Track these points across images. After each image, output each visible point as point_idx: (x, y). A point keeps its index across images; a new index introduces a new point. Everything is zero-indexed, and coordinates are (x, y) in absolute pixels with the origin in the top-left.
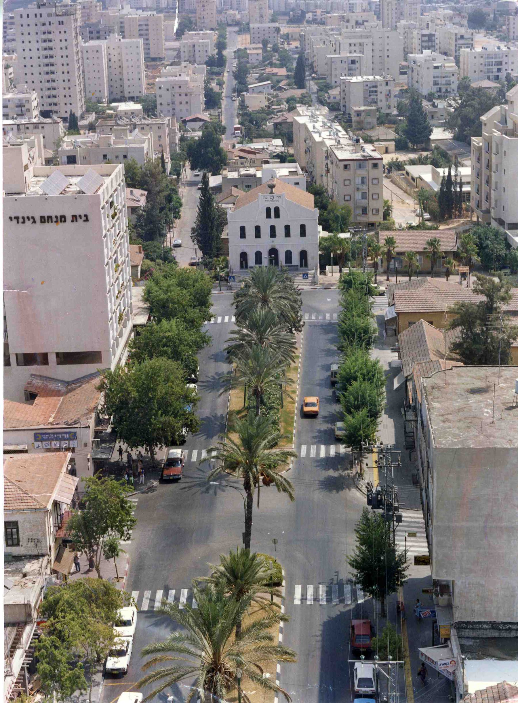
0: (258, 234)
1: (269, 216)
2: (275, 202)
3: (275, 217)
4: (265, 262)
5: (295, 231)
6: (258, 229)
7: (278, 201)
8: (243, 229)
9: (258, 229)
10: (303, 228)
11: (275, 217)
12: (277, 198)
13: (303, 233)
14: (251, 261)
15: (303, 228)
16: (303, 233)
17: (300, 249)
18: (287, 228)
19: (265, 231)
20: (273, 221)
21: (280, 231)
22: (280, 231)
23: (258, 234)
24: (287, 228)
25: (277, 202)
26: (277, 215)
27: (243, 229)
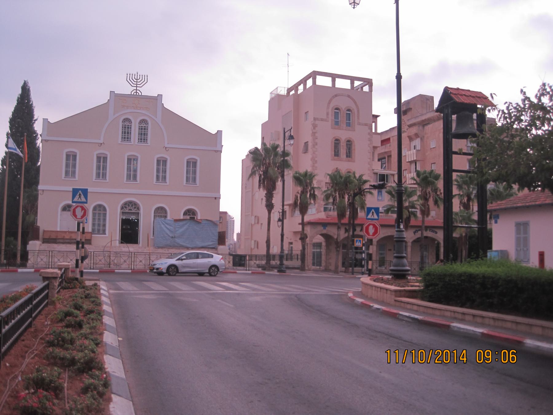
5: (176, 170)
10: (192, 164)
15: (192, 164)
19: (117, 168)
20: (134, 147)
22: (147, 169)
27: (71, 158)
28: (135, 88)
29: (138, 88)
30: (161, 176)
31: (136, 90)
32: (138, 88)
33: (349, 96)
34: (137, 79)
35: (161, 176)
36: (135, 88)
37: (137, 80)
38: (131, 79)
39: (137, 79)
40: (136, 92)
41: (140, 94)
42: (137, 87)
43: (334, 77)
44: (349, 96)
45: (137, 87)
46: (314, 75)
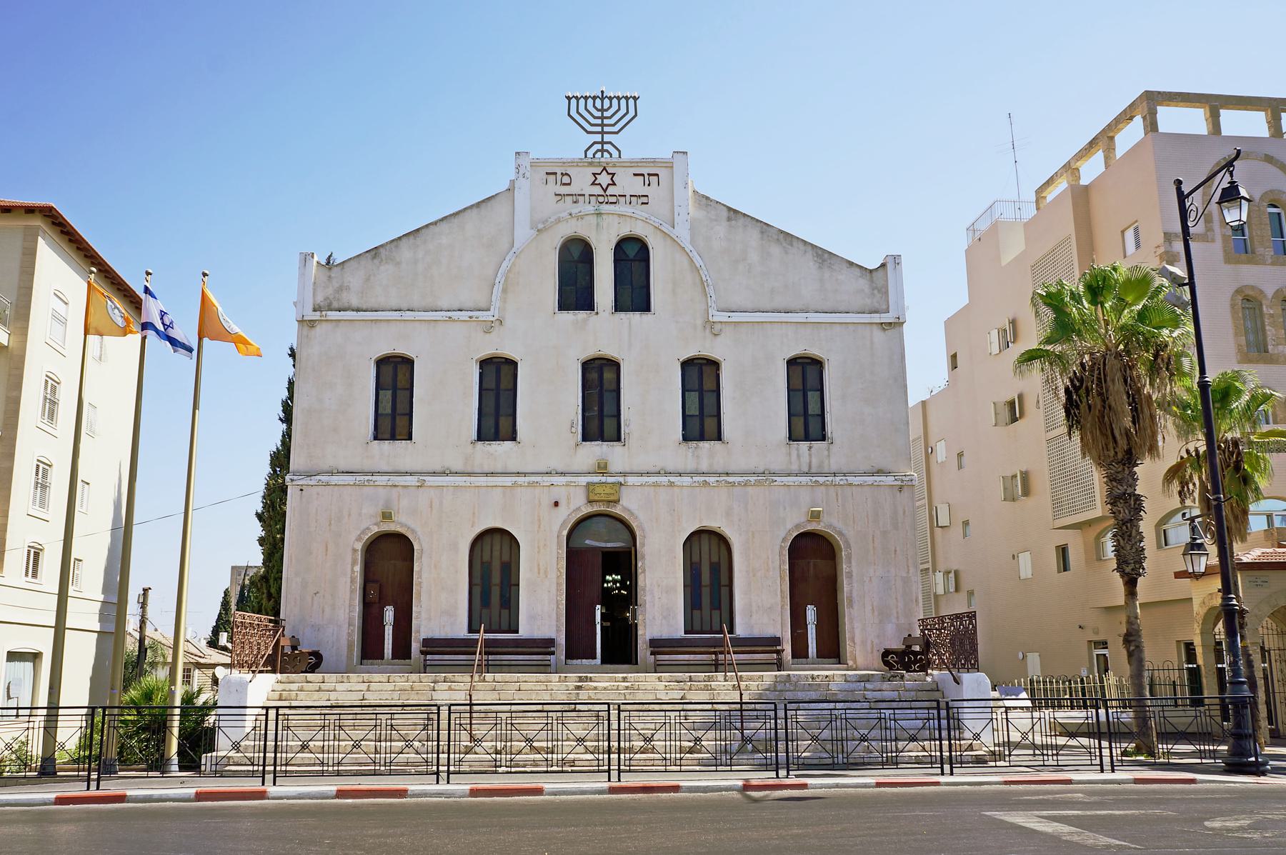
0: (497, 419)
1: (575, 294)
2: (622, 208)
3: (619, 307)
4: (541, 605)
6: (498, 380)
7: (643, 199)
8: (395, 375)
9: (498, 380)
10: (805, 375)
11: (619, 307)
12: (637, 187)
13: (807, 421)
14: (442, 603)
15: (805, 375)
16: (807, 421)
17: (793, 522)
18: (701, 377)
19: (549, 402)
20: (604, 330)
21: (651, 401)
22: (651, 401)
23: (497, 419)
24: (701, 377)
25: (640, 211)
26: (634, 294)
27: (395, 375)
28: (598, 138)
29: (607, 138)
30: (702, 421)
31: (603, 143)
32: (607, 138)
33: (1269, 159)
34: (602, 110)
35: (702, 421)
36: (598, 138)
37: (602, 113)
38: (582, 110)
39: (602, 110)
40: (602, 151)
41: (615, 153)
42: (602, 133)
43: (1214, 104)
44: (1269, 159)
45: (602, 133)
46: (1151, 101)
